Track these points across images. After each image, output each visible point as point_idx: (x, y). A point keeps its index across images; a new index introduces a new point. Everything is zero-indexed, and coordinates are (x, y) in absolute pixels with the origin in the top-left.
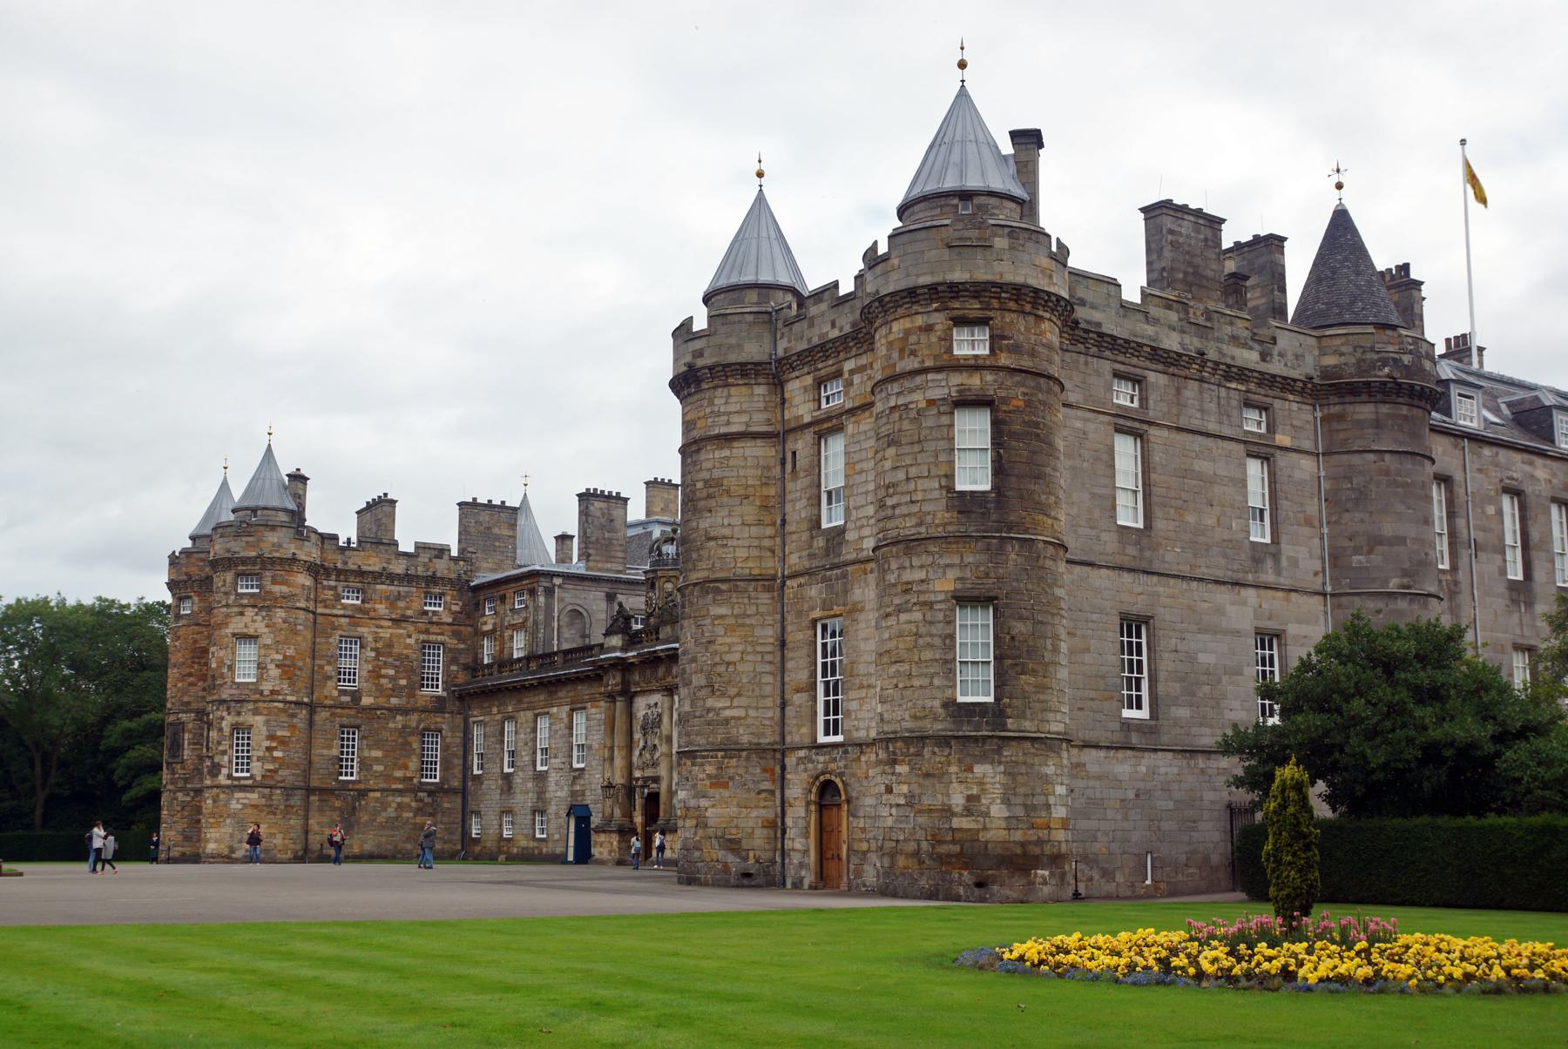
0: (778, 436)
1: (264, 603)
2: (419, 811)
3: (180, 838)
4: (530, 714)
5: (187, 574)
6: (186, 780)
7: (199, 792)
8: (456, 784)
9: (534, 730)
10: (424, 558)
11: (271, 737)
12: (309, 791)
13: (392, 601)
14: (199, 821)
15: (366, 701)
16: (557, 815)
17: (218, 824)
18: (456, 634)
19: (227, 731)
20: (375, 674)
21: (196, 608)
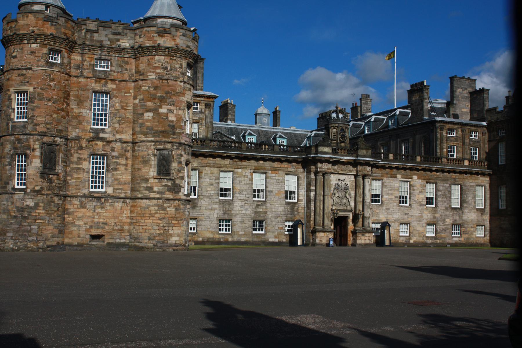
3: (56, 232)
4: (215, 170)
5: (65, 34)
6: (60, 188)
7: (65, 197)
9: (218, 178)
14: (64, 219)
16: (242, 222)
17: (179, 225)
19: (184, 163)
21: (66, 61)
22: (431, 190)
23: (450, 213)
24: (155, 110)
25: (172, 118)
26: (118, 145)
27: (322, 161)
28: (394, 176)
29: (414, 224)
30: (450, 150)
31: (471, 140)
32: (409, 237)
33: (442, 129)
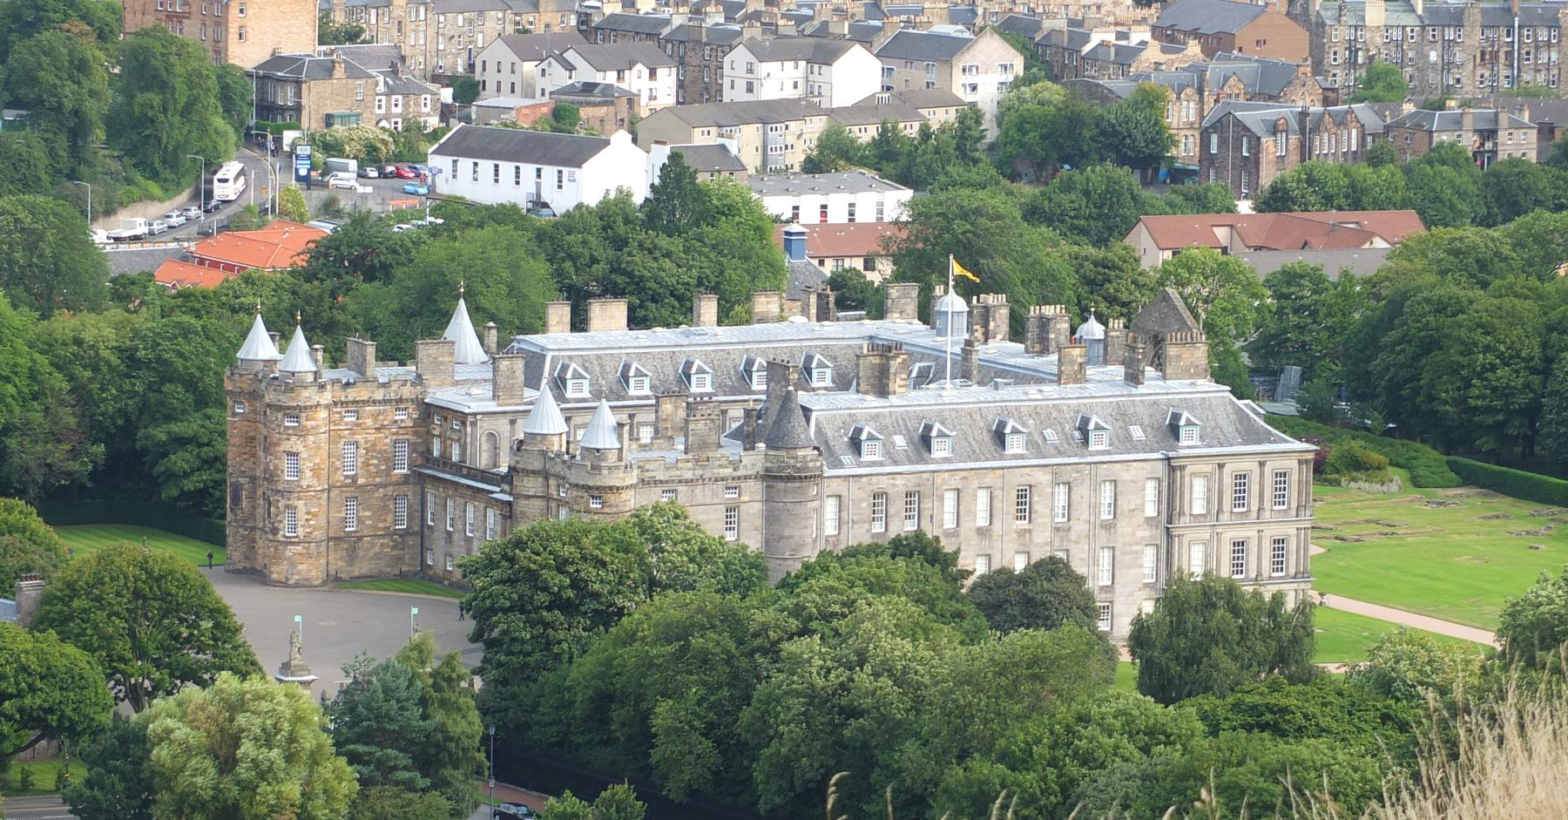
0: (547, 498)
1: (301, 433)
2: (394, 548)
7: (253, 528)
8: (417, 529)
10: (395, 387)
11: (308, 513)
12: (329, 539)
13: (375, 416)
15: (361, 481)
18: (416, 434)
20: (366, 464)
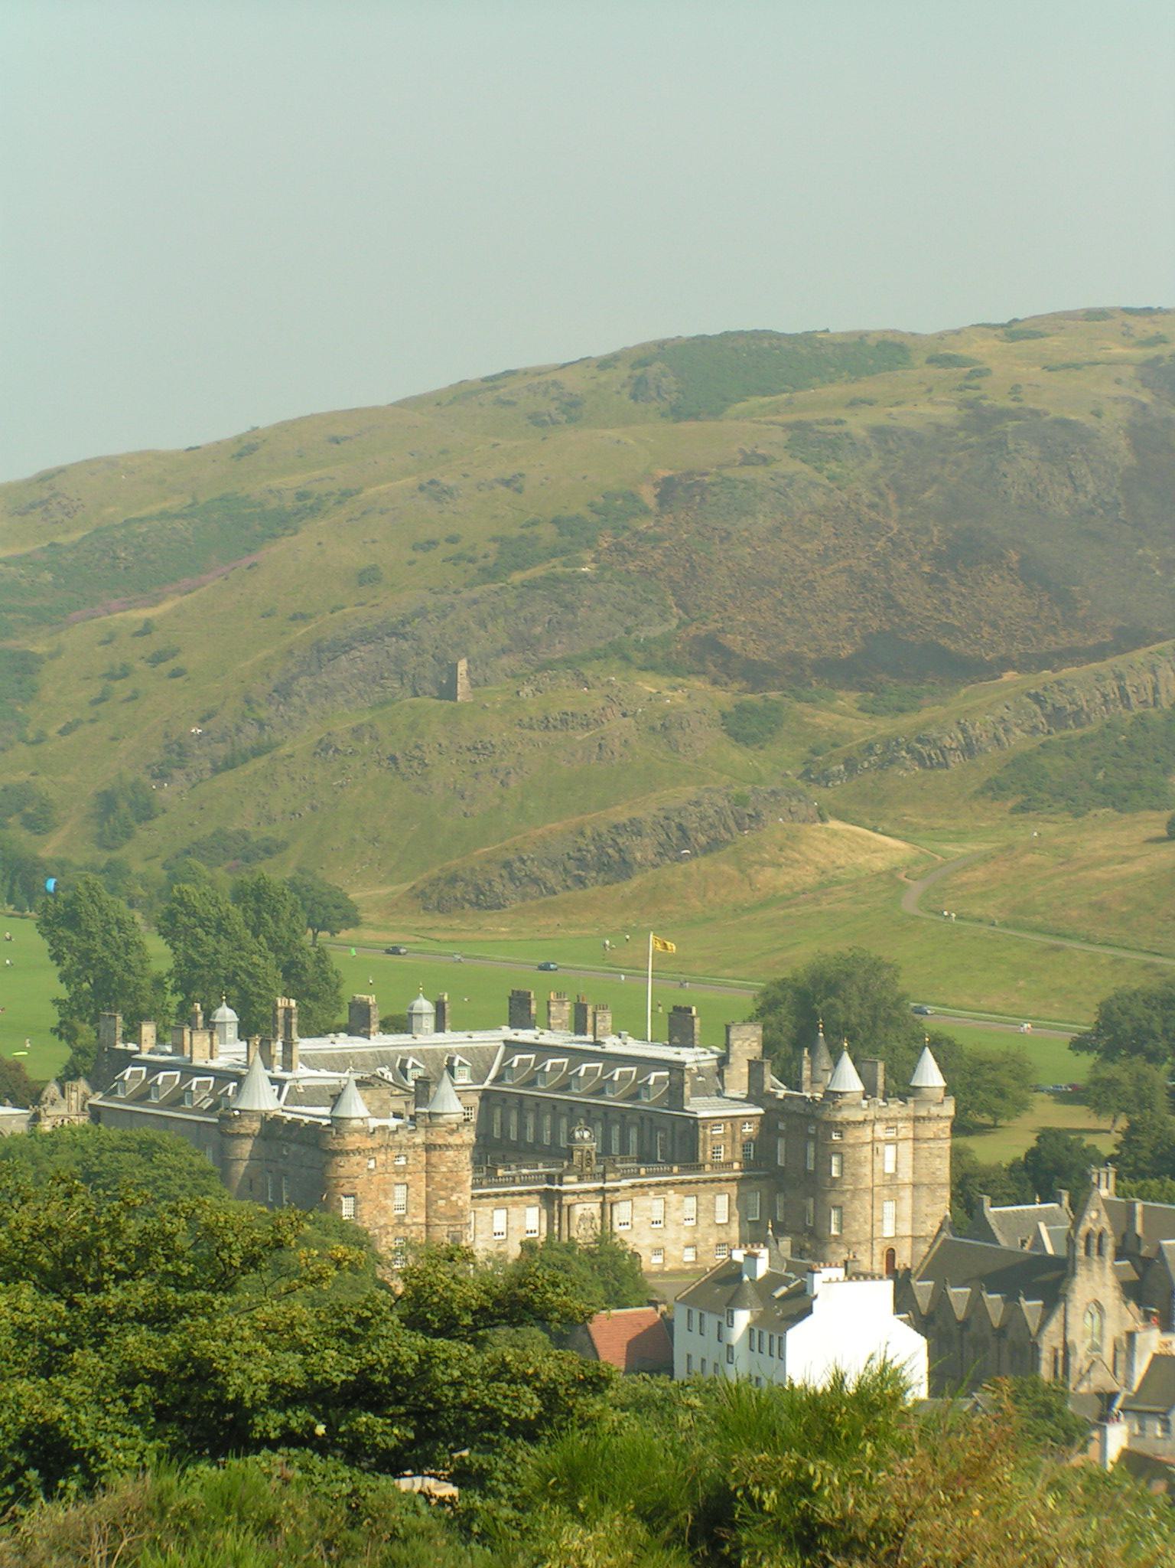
22: (691, 1202)
23: (713, 1230)
24: (447, 1199)
25: (460, 1203)
26: (414, 1228)
27: (566, 1193)
28: (646, 1194)
29: (669, 1248)
30: (716, 1150)
31: (743, 1134)
32: (664, 1264)
33: (705, 1127)
